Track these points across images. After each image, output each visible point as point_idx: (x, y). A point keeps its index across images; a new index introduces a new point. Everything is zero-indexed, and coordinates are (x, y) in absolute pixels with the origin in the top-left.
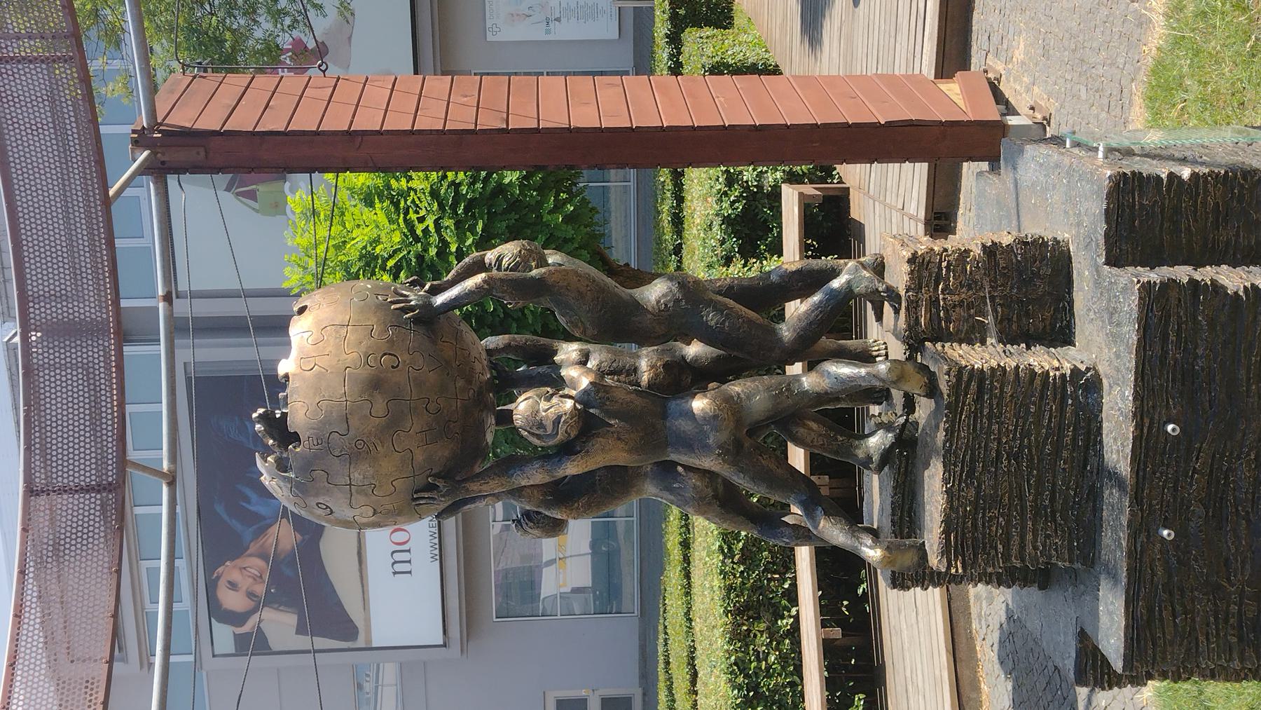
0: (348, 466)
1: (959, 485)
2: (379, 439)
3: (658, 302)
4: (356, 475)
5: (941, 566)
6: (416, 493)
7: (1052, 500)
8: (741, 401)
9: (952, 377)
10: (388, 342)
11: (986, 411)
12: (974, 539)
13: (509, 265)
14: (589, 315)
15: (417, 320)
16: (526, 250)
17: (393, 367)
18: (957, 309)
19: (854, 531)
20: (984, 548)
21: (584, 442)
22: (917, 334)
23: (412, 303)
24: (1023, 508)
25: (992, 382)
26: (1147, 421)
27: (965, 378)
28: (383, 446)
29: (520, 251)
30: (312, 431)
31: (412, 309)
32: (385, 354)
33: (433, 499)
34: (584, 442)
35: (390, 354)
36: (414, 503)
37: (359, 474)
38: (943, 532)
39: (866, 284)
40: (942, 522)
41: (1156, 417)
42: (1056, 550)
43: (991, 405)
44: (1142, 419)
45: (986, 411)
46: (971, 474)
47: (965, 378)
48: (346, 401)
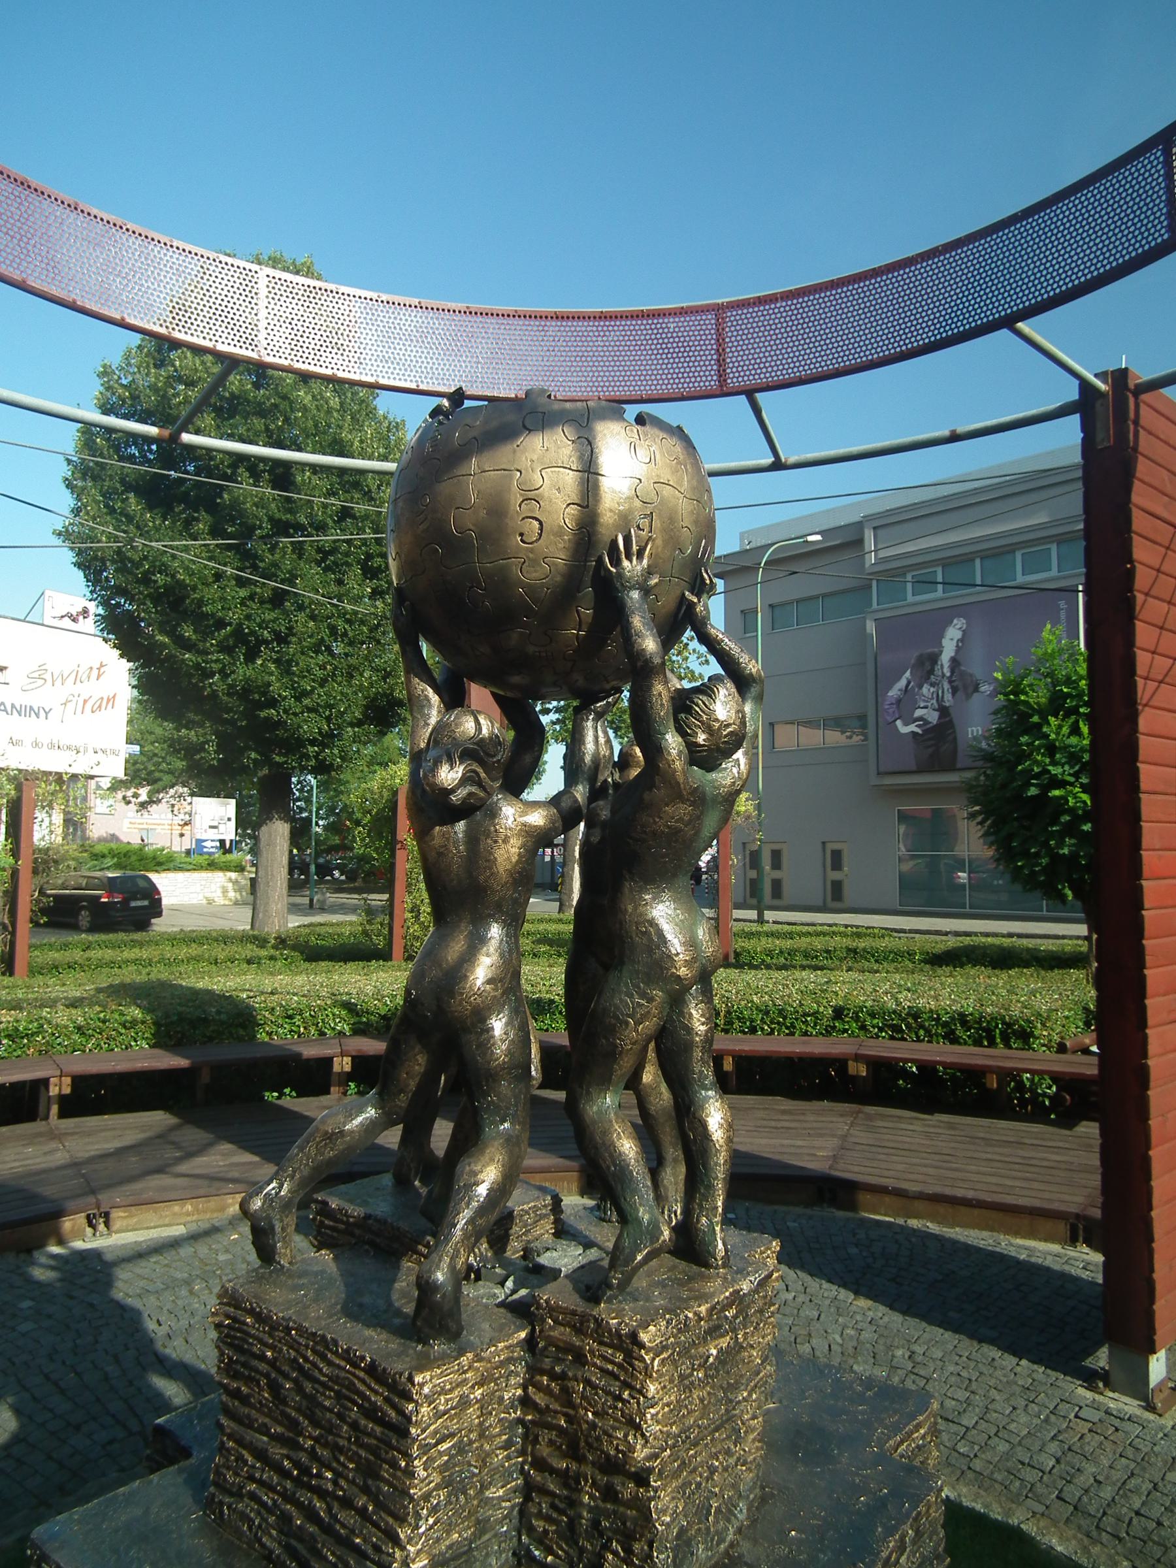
3: (652, 923)
10: (561, 527)
13: (697, 705)
16: (719, 728)
23: (626, 563)
29: (717, 720)
31: (616, 562)
32: (541, 523)
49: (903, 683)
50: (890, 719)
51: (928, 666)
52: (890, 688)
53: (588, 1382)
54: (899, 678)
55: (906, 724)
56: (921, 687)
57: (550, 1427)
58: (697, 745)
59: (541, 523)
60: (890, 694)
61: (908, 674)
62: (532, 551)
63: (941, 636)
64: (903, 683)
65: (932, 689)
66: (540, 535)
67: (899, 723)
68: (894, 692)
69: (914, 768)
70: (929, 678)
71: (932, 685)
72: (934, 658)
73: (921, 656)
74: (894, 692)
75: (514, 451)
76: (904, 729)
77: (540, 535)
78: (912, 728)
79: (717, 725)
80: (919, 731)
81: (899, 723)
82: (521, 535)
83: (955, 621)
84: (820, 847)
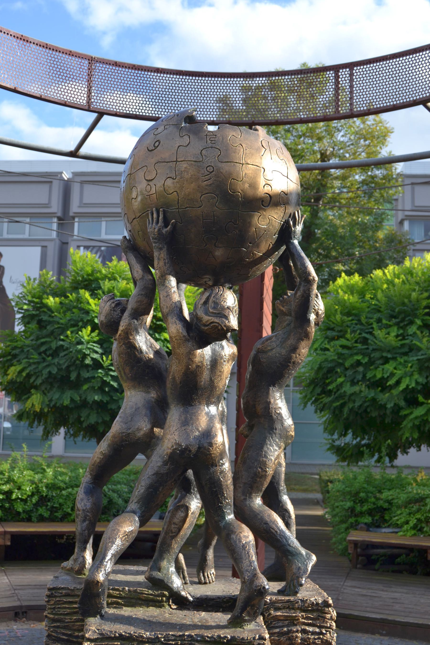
0: (193, 160)
2: (213, 183)
4: (185, 166)
5: (90, 633)
6: (164, 211)
8: (220, 466)
9: (258, 641)
14: (277, 355)
21: (195, 339)
22: (268, 609)
28: (207, 185)
30: (221, 138)
33: (157, 222)
34: (195, 339)
35: (270, 201)
36: (154, 209)
37: (185, 168)
38: (121, 635)
39: (302, 568)
40: (130, 634)
48: (243, 164)
53: (304, 631)
75: (261, 158)
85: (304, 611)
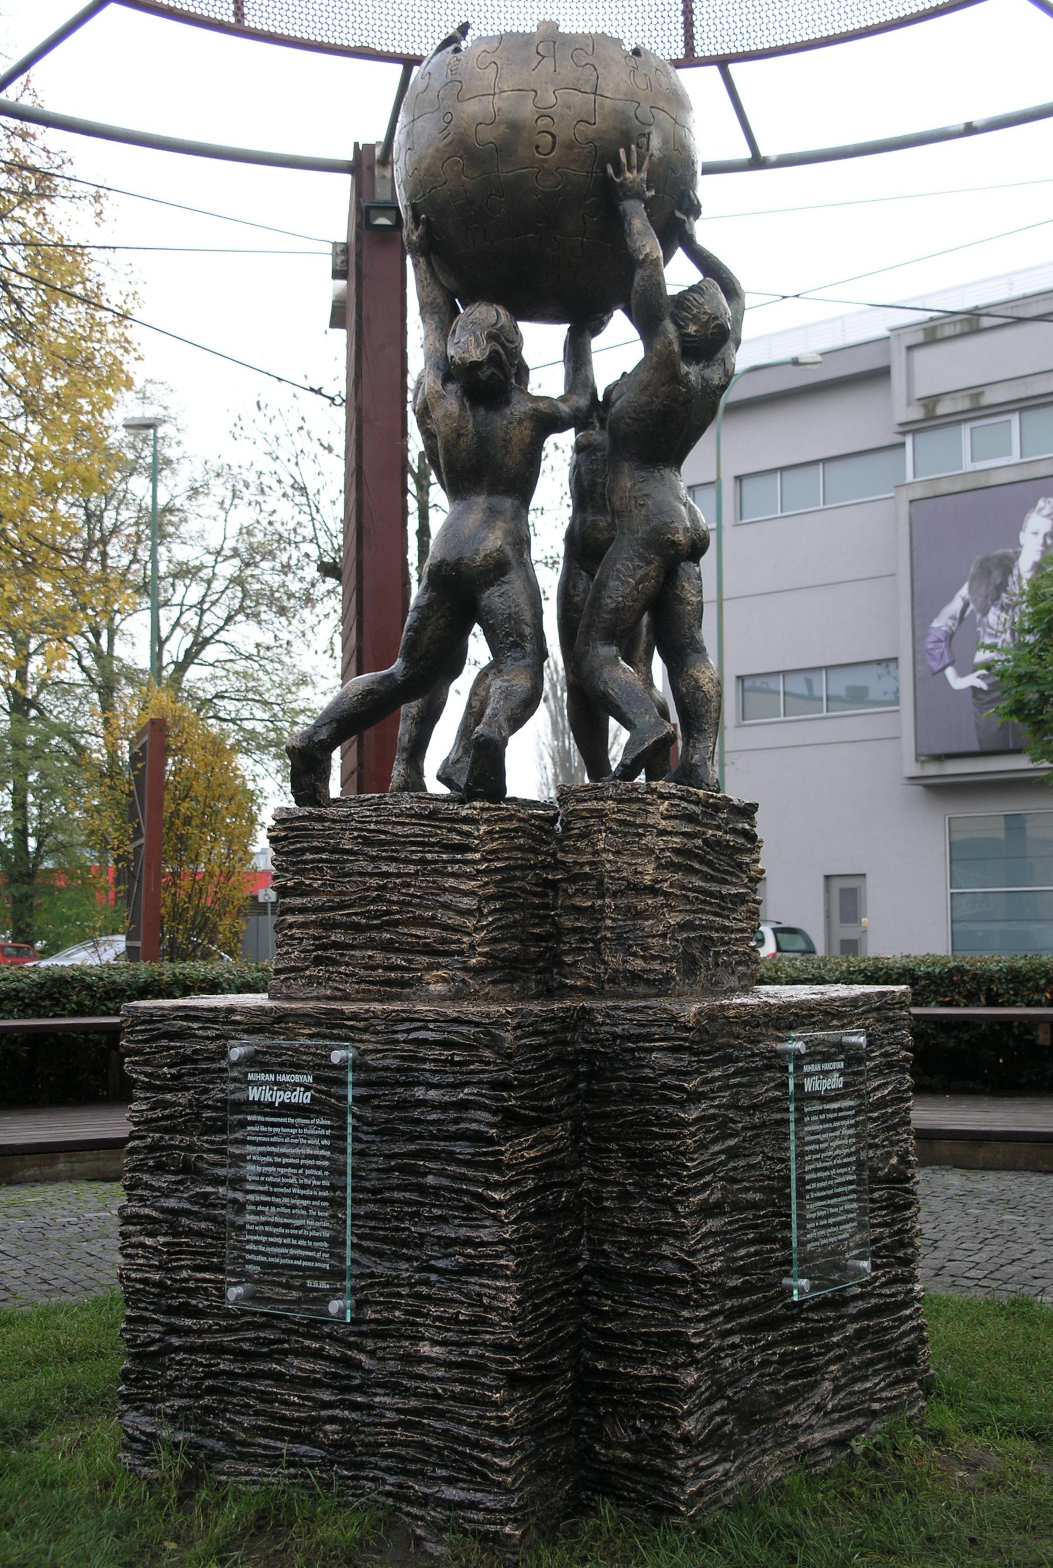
1: (356, 829)
7: (335, 945)
11: (429, 856)
12: (303, 851)
15: (607, 181)
17: (537, 147)
18: (590, 849)
19: (337, 721)
20: (293, 864)
24: (331, 909)
25: (458, 861)
26: (361, 1024)
27: (465, 828)
31: (619, 172)
32: (553, 136)
41: (365, 1037)
42: (287, 953)
43: (435, 862)
44: (366, 1019)
45: (429, 856)
46: (368, 842)
47: (465, 828)
49: (955, 606)
50: (936, 666)
51: (996, 577)
52: (935, 615)
53: (609, 830)
54: (950, 598)
55: (962, 673)
56: (985, 613)
57: (573, 879)
58: (688, 335)
59: (553, 136)
60: (936, 624)
61: (964, 591)
62: (546, 161)
63: (1018, 526)
64: (955, 606)
65: (1003, 615)
66: (553, 147)
67: (950, 672)
68: (942, 622)
69: (975, 747)
70: (999, 597)
71: (1004, 608)
72: (1007, 564)
73: (987, 559)
74: (942, 622)
76: (959, 683)
77: (553, 147)
78: (973, 680)
79: (706, 317)
80: (983, 685)
81: (950, 672)
82: (537, 147)
83: (1041, 503)
84: (821, 883)
85: (620, 801)
